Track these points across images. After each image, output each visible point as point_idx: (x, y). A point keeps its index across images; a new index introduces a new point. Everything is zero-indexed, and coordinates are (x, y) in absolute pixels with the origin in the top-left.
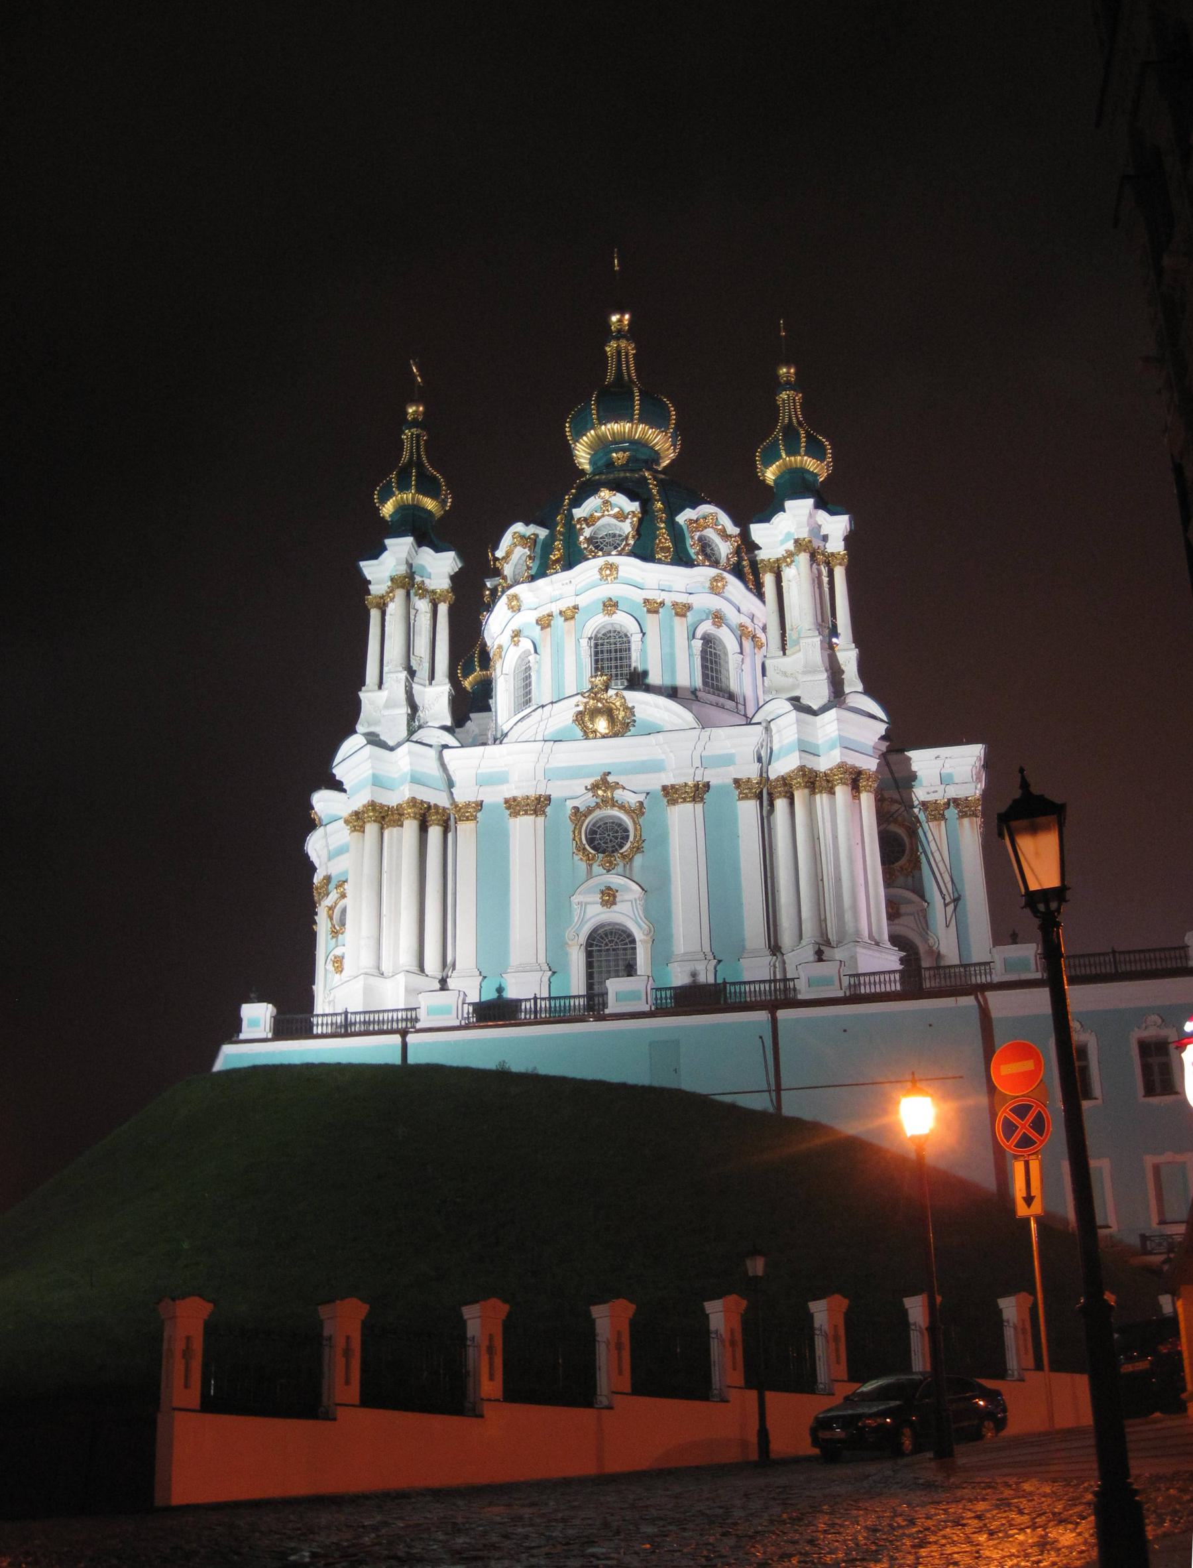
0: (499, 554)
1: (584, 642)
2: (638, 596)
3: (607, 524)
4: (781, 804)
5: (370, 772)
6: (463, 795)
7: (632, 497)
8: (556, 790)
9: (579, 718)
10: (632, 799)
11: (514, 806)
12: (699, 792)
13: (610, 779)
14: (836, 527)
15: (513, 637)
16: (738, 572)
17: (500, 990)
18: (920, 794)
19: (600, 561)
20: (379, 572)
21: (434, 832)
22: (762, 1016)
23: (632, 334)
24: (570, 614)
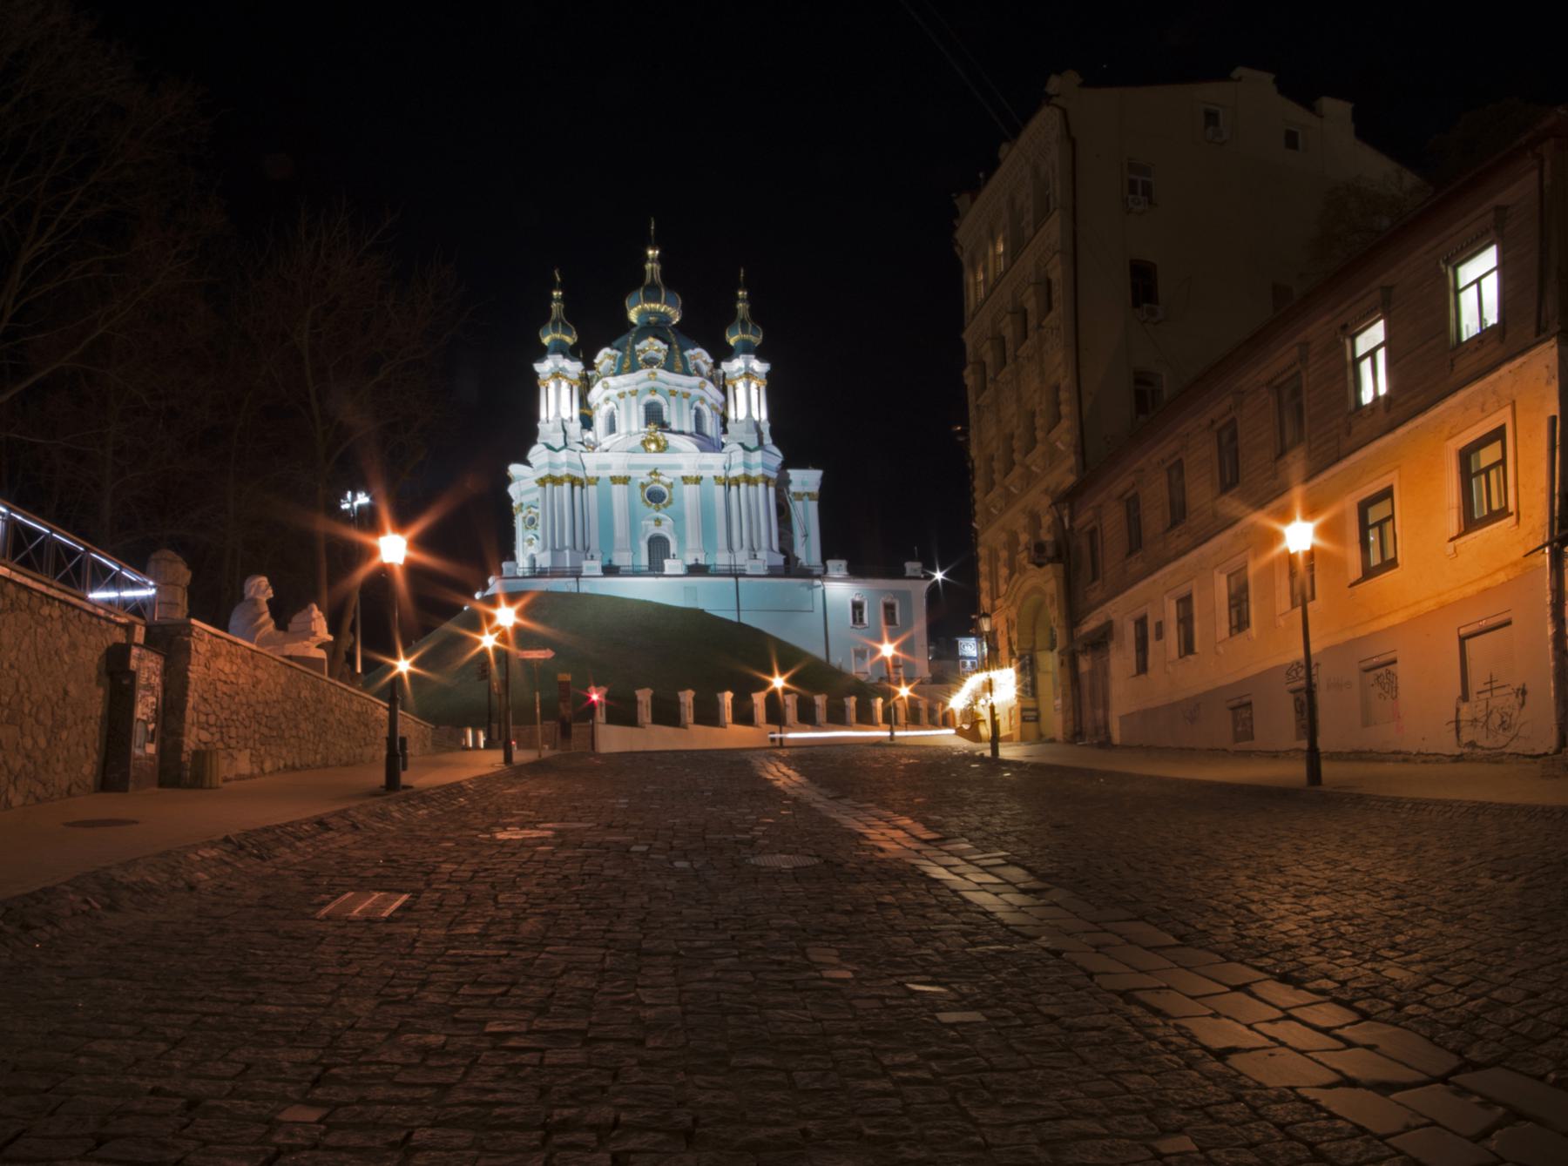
3: (652, 353)
4: (734, 488)
6: (590, 473)
7: (664, 342)
8: (633, 473)
9: (643, 443)
10: (668, 481)
11: (614, 480)
12: (698, 480)
14: (760, 367)
16: (711, 379)
18: (792, 488)
21: (577, 488)
22: (732, 580)
23: (660, 259)
24: (634, 393)
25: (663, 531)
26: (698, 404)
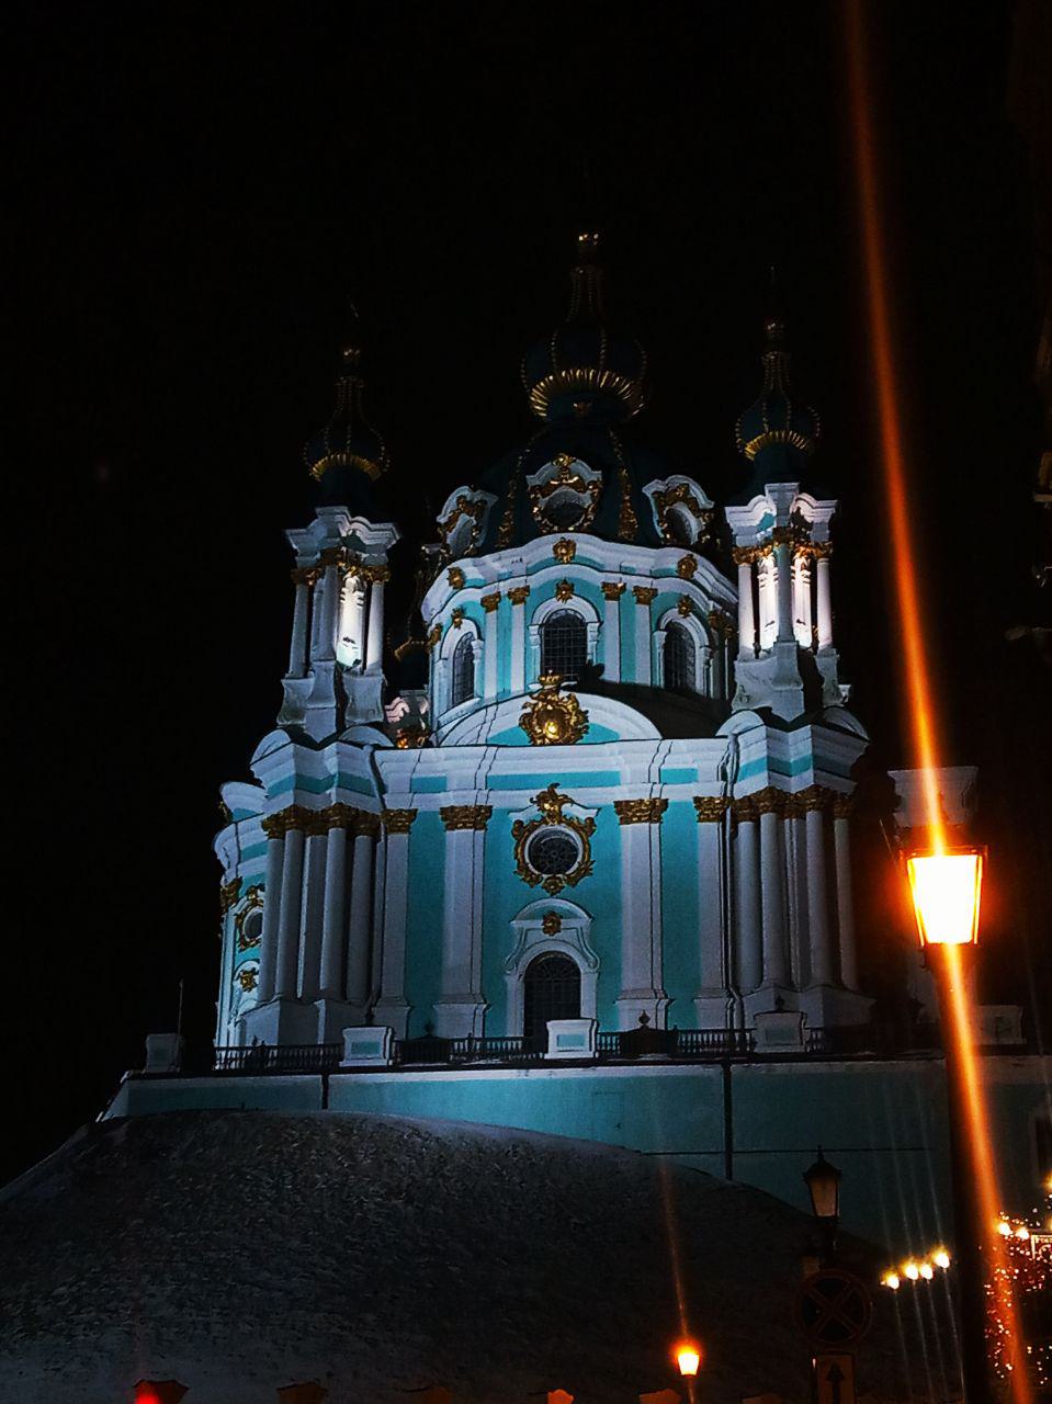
0: (442, 519)
1: (534, 629)
2: (598, 578)
3: (565, 491)
4: (745, 827)
5: (293, 772)
6: (394, 802)
8: (498, 800)
9: (526, 721)
10: (583, 815)
11: (452, 817)
12: (654, 810)
13: (558, 791)
15: (454, 618)
17: (430, 1027)
19: (555, 538)
20: (306, 541)
21: (362, 841)
22: (713, 1071)
24: (519, 596)
25: (565, 944)
26: (673, 614)
